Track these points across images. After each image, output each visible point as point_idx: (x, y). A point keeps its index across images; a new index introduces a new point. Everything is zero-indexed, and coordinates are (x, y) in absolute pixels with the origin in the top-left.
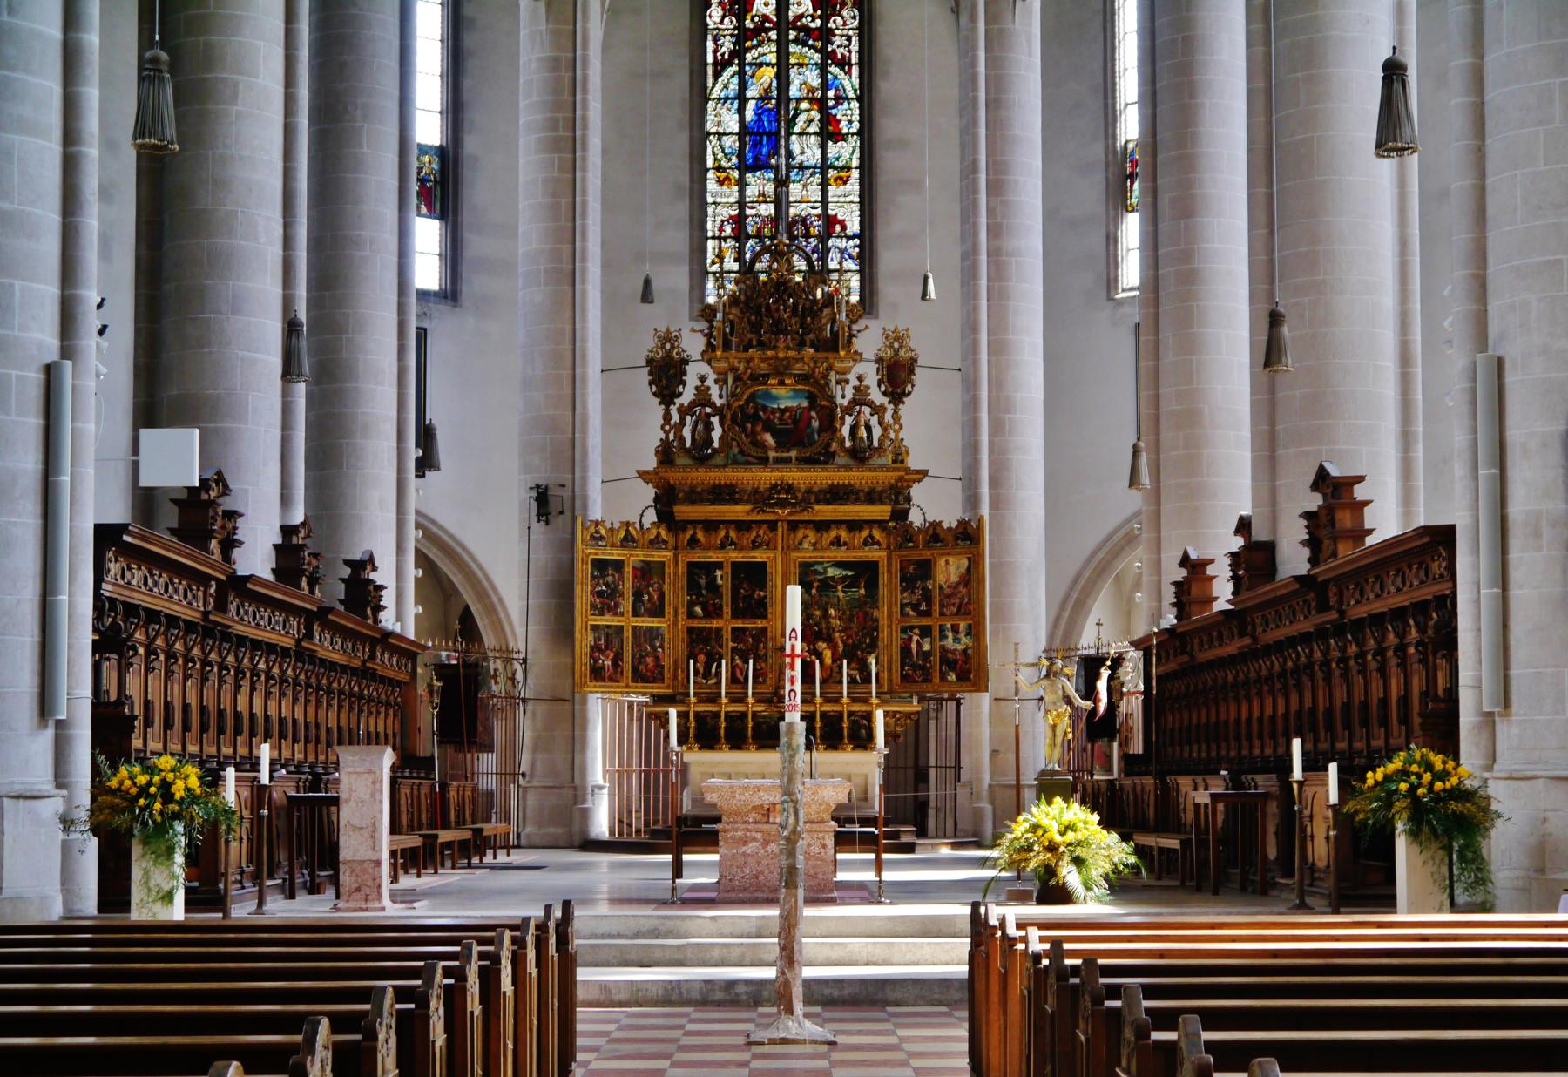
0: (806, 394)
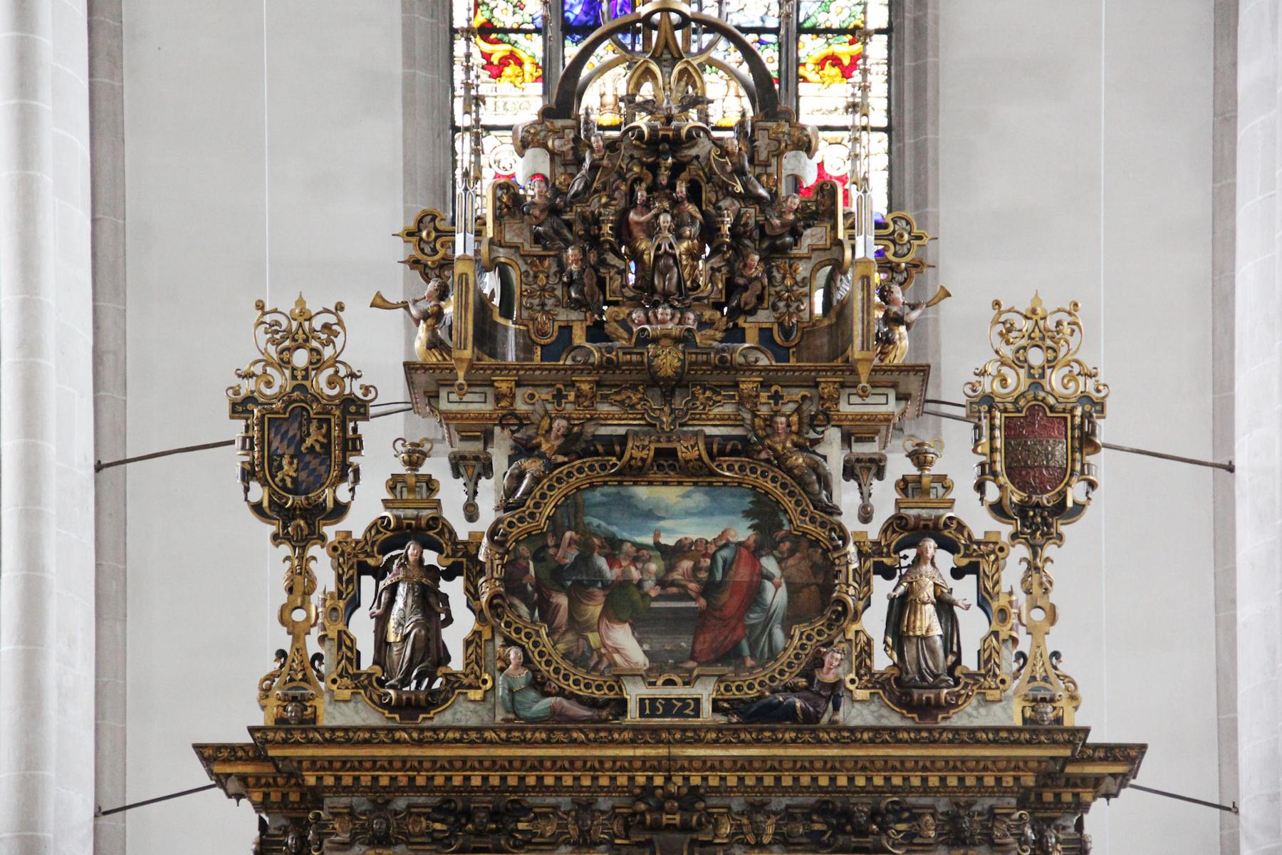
0: (747, 502)
